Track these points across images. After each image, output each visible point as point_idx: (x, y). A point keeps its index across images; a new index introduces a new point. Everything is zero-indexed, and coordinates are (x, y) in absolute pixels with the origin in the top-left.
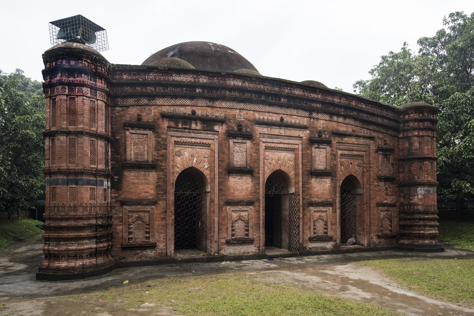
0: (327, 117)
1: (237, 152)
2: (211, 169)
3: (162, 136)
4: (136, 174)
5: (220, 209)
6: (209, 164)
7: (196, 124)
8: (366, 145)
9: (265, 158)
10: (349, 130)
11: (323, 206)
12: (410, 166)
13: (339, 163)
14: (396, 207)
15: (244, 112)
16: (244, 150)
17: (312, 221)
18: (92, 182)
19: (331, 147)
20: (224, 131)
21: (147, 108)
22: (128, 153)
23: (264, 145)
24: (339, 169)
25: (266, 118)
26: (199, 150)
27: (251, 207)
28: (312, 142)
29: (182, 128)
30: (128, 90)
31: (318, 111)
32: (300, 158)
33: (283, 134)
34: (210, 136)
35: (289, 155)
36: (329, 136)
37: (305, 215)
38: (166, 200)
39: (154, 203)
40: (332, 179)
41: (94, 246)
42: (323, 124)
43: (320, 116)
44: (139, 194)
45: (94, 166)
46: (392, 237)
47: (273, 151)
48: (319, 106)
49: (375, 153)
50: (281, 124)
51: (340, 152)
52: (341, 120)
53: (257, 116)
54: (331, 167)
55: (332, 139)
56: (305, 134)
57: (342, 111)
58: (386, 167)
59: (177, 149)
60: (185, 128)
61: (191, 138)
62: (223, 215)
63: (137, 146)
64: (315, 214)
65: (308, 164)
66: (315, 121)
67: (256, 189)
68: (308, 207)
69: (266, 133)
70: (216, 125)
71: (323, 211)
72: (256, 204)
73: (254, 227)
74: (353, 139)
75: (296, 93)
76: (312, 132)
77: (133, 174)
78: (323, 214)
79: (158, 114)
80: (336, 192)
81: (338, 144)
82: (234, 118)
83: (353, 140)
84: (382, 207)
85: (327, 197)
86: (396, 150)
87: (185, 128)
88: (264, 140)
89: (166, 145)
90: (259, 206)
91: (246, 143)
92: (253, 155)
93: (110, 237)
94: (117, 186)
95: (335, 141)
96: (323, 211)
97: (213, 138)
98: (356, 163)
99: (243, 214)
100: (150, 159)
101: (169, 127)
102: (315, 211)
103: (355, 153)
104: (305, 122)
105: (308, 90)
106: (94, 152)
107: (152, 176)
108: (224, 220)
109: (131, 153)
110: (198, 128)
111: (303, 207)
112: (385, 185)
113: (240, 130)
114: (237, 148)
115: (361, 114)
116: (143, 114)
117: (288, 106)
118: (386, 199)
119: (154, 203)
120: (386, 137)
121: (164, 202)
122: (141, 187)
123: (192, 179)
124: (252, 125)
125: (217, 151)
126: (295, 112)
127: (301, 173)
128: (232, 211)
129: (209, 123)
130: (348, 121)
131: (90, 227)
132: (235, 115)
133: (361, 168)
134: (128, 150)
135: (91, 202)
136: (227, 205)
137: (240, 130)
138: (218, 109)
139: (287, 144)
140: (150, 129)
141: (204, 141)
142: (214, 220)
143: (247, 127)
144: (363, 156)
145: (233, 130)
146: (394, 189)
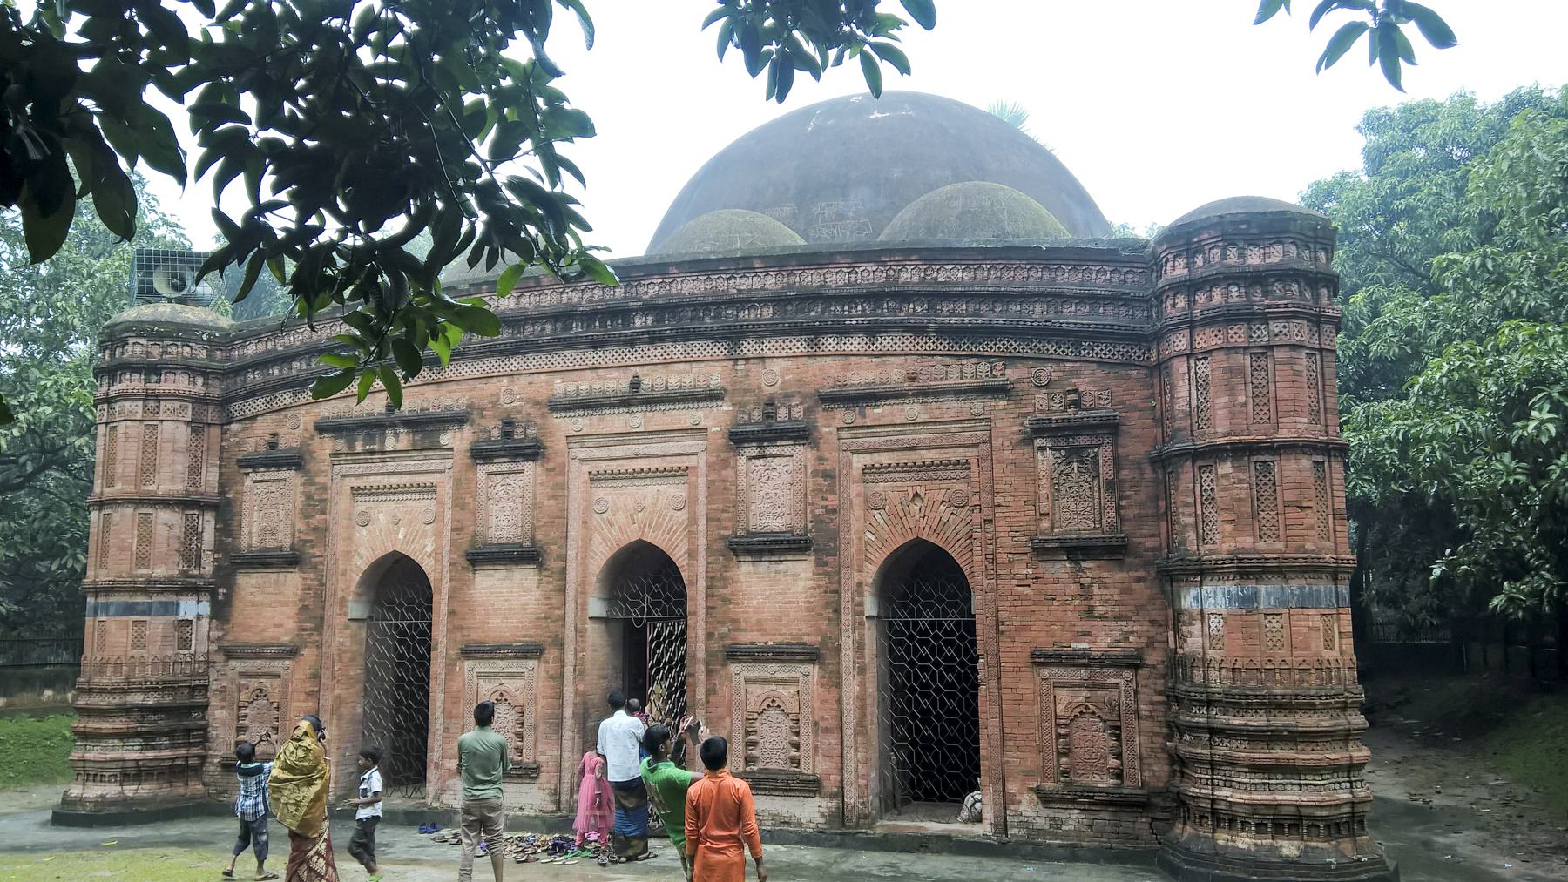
0: (798, 345)
2: (437, 553)
3: (317, 480)
5: (450, 667)
7: (396, 435)
8: (974, 419)
9: (588, 509)
10: (894, 374)
11: (782, 661)
13: (857, 501)
14: (1143, 672)
15: (524, 380)
16: (519, 492)
17: (737, 713)
18: (140, 608)
19: (815, 445)
20: (466, 445)
21: (291, 413)
22: (245, 531)
23: (586, 468)
24: (856, 524)
25: (584, 387)
26: (412, 503)
27: (533, 663)
28: (738, 439)
29: (364, 453)
30: (254, 377)
31: (760, 332)
32: (702, 499)
33: (641, 429)
34: (434, 464)
35: (673, 491)
36: (808, 411)
37: (715, 692)
38: (319, 646)
39: (291, 652)
40: (820, 563)
41: (135, 755)
42: (785, 372)
43: (770, 346)
44: (264, 630)
45: (145, 571)
46: (1120, 804)
47: (619, 483)
48: (768, 312)
49: (1015, 446)
50: (635, 398)
51: (859, 461)
52: (856, 343)
53: (561, 387)
54: (817, 520)
55: (820, 417)
56: (717, 418)
57: (857, 314)
58: (1079, 498)
59: (361, 507)
60: (372, 452)
61: (389, 474)
62: (455, 687)
63: (267, 510)
64: (756, 689)
66: (755, 367)
67: (551, 607)
68: (724, 665)
69: (584, 432)
70: (445, 431)
71: (784, 681)
72: (551, 654)
73: (542, 727)
74: (907, 408)
75: (686, 291)
76: (740, 406)
77: (253, 582)
78: (784, 692)
79: (311, 427)
80: (837, 611)
81: (846, 434)
82: (495, 403)
83: (913, 409)
84: (1055, 670)
85: (798, 626)
87: (372, 452)
90: (562, 662)
91: (521, 472)
92: (546, 502)
93: (202, 735)
94: (221, 612)
95: (829, 423)
96: (784, 681)
97: (441, 467)
99: (510, 685)
100: (287, 543)
101: (335, 455)
102: (748, 680)
103: (927, 456)
104: (715, 375)
106: (146, 539)
107: (292, 582)
108: (456, 701)
110: (400, 446)
111: (708, 664)
112: (1077, 574)
113: (507, 435)
115: (946, 308)
116: (282, 432)
117: (653, 339)
118: (1086, 634)
119: (291, 652)
120: (1078, 376)
121: (315, 651)
122: (268, 612)
123: (398, 585)
124: (543, 416)
125: (449, 504)
126: (676, 350)
128: (479, 675)
129: (427, 427)
130: (885, 342)
131: (125, 710)
133: (964, 512)
134: (245, 523)
135: (135, 653)
136: (469, 658)
138: (453, 387)
139: (657, 456)
140: (289, 466)
141: (421, 479)
143: (529, 423)
144: (967, 462)
146: (1125, 591)
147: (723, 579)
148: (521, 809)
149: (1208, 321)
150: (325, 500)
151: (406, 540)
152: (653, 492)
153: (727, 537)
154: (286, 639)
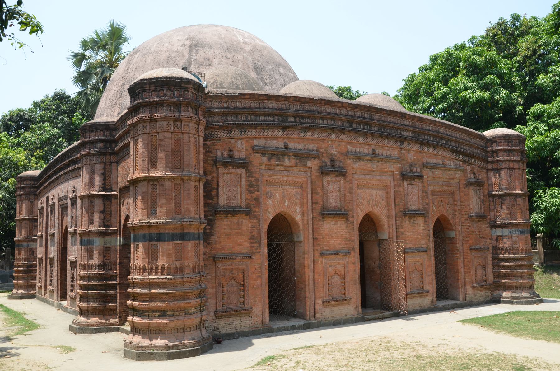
0: (417, 147)
1: (331, 192)
3: (255, 175)
4: (229, 223)
6: (300, 207)
7: (289, 159)
12: (502, 203)
16: (337, 189)
23: (356, 182)
32: (393, 197)
35: (380, 193)
36: (421, 169)
44: (233, 247)
51: (431, 188)
52: (431, 150)
60: (278, 165)
65: (401, 204)
70: (309, 160)
86: (486, 184)
87: (278, 165)
88: (356, 176)
89: (259, 185)
92: (347, 194)
98: (447, 201)
100: (244, 205)
103: (446, 188)
104: (396, 153)
105: (398, 117)
107: (246, 223)
109: (225, 197)
110: (291, 164)
114: (331, 188)
117: (381, 136)
125: (309, 191)
126: (386, 142)
127: (394, 215)
129: (301, 157)
130: (437, 152)
132: (327, 147)
137: (333, 165)
142: (309, 276)
145: (326, 166)
147: (402, 226)
148: (346, 315)
149: (514, 161)
150: (259, 185)
151: (288, 207)
152: (374, 192)
153: (401, 211)
154: (245, 251)
